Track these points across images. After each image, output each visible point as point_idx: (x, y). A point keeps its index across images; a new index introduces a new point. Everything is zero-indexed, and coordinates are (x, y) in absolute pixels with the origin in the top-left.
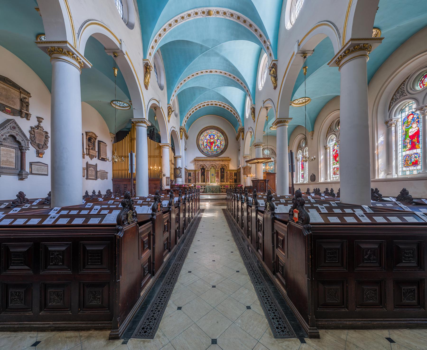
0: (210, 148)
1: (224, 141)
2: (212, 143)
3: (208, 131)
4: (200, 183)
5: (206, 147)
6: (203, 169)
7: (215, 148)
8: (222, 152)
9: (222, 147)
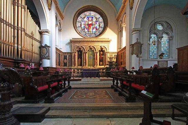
0: (88, 30)
1: (103, 23)
2: (89, 25)
3: (85, 13)
4: (76, 67)
5: (84, 29)
6: (80, 52)
8: (101, 34)
9: (101, 29)
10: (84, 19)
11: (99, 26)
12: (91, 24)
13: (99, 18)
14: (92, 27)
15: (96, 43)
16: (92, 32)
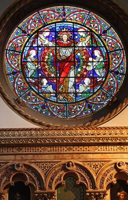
1: (122, 54)
2: (62, 65)
5: (38, 83)
7: (82, 88)
10: (37, 37)
11: (107, 66)
12: (67, 59)
13: (105, 32)
14: (72, 74)
15: (91, 149)
16: (71, 95)
